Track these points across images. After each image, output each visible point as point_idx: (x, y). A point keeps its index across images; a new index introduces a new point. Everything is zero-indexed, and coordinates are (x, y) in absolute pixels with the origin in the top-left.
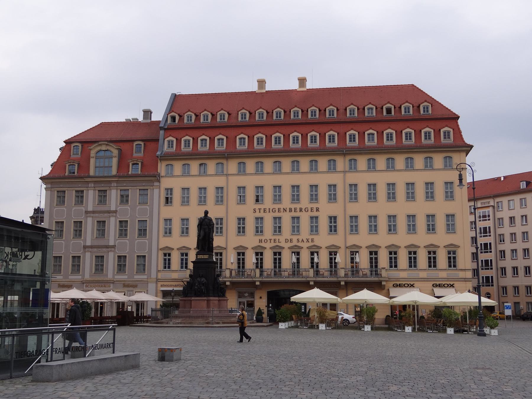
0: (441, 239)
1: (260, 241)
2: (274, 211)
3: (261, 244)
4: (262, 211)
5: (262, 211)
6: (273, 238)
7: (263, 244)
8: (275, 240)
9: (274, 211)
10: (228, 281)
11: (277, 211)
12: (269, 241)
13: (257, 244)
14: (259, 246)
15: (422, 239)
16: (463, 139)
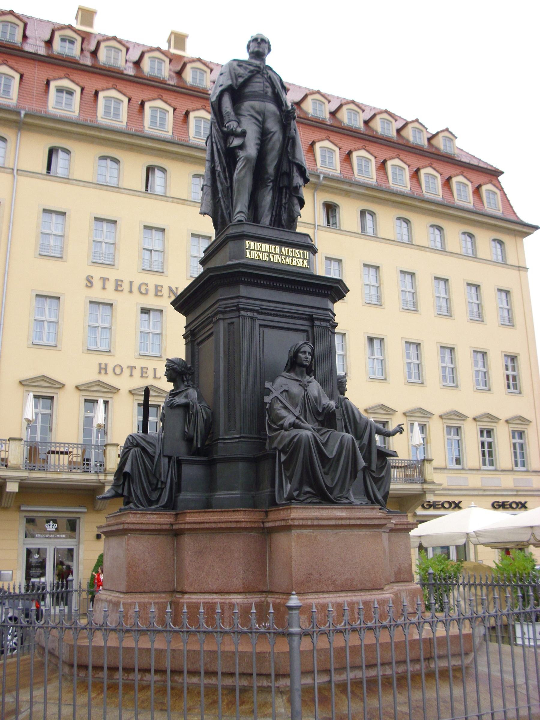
0: (501, 404)
1: (103, 369)
2: (143, 290)
3: (104, 378)
4: (111, 285)
5: (111, 285)
6: (140, 363)
7: (110, 379)
8: (144, 372)
9: (143, 290)
10: (13, 479)
11: (152, 291)
12: (127, 372)
13: (92, 376)
14: (99, 383)
15: (470, 402)
16: (515, 213)
